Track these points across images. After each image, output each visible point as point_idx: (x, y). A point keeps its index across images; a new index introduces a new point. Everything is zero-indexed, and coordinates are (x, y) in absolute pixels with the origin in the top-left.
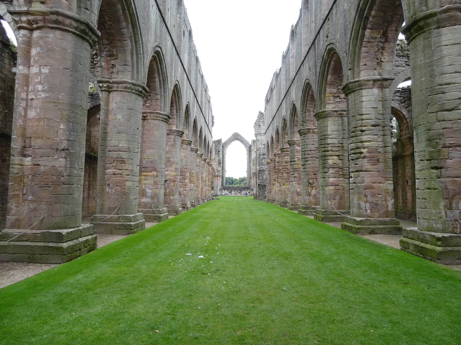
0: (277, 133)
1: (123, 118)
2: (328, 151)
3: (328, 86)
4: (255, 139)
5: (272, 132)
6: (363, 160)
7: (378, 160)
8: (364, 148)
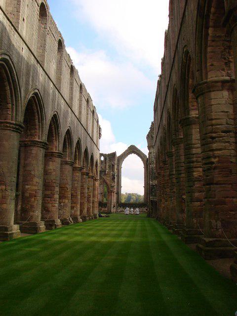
2: (193, 162)
6: (216, 171)
7: (231, 171)
8: (215, 157)
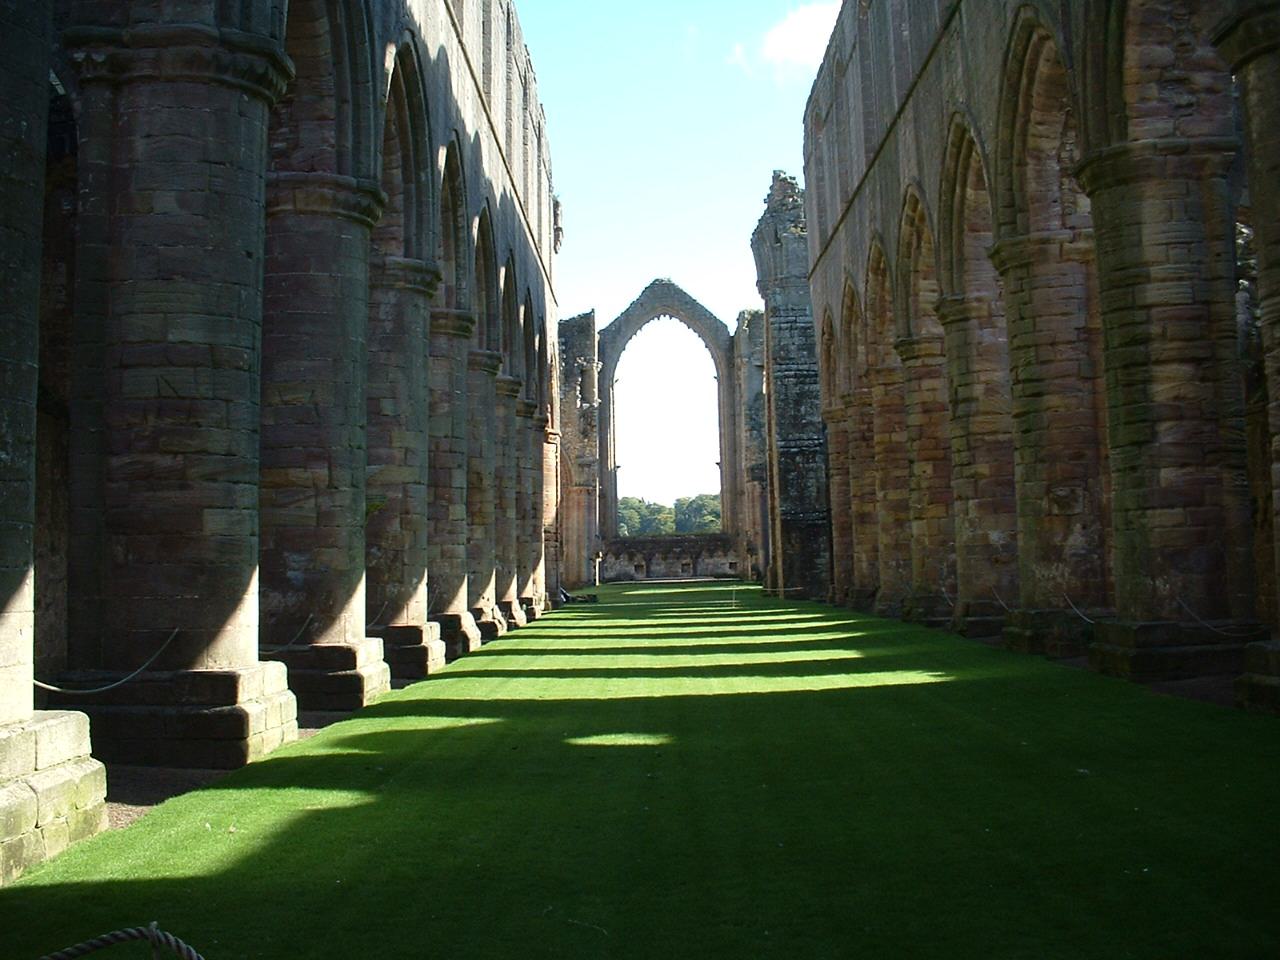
0: (879, 270)
1: (182, 203)
3: (1131, 32)
4: (758, 304)
5: (849, 263)
